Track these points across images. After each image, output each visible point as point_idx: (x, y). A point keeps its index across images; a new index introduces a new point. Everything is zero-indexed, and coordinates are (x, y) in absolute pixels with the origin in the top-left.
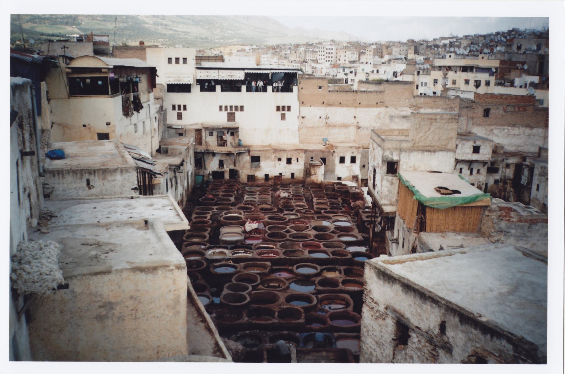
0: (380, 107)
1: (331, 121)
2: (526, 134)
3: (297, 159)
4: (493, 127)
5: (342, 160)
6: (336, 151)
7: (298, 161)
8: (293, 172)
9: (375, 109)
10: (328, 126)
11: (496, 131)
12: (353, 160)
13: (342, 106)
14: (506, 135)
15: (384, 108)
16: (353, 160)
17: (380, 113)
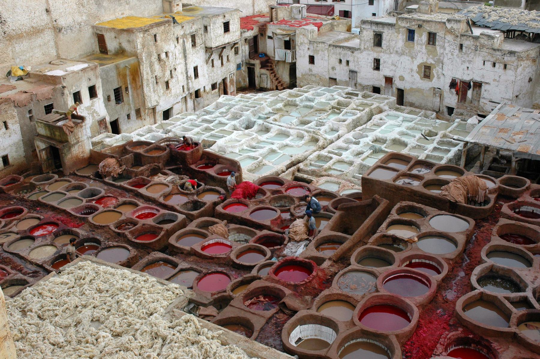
3: (5, 123)
5: (77, 97)
6: (65, 85)
7: (7, 128)
8: (4, 154)
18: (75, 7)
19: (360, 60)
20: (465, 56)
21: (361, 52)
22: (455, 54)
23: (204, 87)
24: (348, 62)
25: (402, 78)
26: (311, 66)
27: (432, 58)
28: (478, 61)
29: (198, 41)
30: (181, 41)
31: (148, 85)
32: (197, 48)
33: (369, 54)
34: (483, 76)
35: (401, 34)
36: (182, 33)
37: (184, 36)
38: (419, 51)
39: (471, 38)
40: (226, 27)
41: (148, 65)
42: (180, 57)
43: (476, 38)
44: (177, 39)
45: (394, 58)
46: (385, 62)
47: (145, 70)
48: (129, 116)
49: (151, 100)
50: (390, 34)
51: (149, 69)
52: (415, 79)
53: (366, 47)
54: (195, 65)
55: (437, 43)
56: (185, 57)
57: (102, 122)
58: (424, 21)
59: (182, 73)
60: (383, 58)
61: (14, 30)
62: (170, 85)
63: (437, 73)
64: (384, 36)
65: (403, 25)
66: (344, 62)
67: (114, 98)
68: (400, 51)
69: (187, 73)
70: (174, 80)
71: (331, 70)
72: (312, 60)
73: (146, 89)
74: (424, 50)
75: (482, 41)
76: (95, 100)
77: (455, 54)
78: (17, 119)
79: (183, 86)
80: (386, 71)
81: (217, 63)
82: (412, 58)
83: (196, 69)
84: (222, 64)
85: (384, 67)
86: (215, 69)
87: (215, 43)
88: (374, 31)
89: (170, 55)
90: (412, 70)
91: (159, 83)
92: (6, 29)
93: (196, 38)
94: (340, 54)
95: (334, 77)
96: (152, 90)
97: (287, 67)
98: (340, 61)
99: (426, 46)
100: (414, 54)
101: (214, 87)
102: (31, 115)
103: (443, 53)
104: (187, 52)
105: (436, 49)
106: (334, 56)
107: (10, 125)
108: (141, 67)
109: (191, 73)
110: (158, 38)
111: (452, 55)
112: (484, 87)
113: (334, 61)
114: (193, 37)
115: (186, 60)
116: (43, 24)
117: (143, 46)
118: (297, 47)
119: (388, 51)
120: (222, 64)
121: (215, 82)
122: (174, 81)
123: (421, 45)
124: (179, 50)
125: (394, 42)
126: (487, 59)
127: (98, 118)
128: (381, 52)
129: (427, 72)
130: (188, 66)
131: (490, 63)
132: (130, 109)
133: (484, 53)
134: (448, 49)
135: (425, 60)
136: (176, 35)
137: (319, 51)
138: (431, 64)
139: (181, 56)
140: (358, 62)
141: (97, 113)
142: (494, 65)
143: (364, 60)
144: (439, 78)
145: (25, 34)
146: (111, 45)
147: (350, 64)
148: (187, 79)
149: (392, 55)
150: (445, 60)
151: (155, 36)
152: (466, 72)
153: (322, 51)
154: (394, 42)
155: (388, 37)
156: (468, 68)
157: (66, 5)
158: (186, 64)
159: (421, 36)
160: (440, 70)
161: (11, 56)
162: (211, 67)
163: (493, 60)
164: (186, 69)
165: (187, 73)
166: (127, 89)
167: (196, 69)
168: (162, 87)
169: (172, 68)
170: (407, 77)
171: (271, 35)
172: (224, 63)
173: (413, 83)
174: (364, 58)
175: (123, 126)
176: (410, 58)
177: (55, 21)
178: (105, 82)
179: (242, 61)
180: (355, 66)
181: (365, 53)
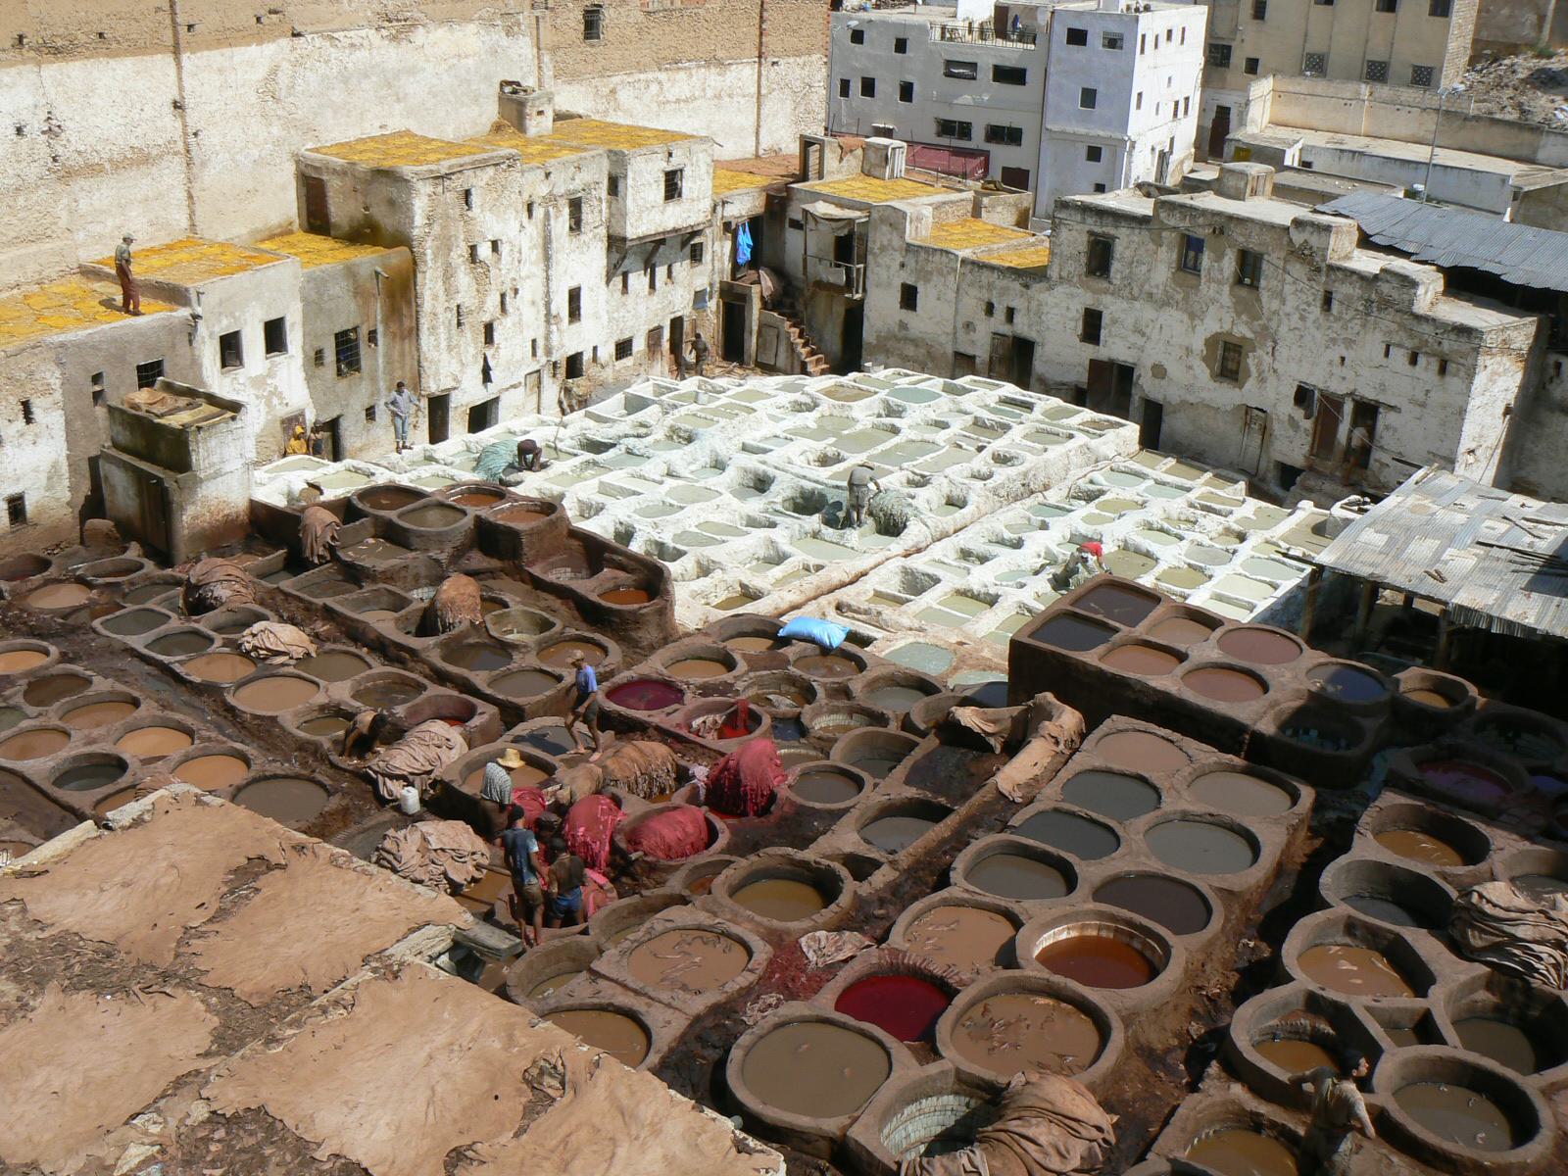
0: (274, 38)
1: (76, 141)
2: (710, 93)
3: (26, 407)
4: (615, 80)
5: (230, 348)
6: (199, 310)
7: (29, 419)
9: (253, 50)
10: (63, 172)
11: (625, 96)
12: (275, 336)
13: (112, 54)
14: (654, 106)
15: (285, 42)
16: (275, 336)
17: (274, 72)
18: (253, 99)
19: (1045, 309)
20: (1337, 326)
21: (1051, 288)
22: (1312, 317)
23: (595, 349)
24: (1010, 313)
25: (1159, 371)
26: (906, 315)
27: (1247, 323)
28: (1372, 344)
29: (588, 216)
30: (539, 212)
31: (433, 329)
32: (583, 237)
33: (1072, 295)
34: (1383, 388)
35: (1164, 248)
36: (543, 190)
37: (551, 199)
38: (1213, 301)
39: (1355, 277)
40: (672, 187)
41: (440, 273)
42: (533, 258)
43: (1369, 281)
44: (530, 208)
45: (1146, 312)
46: (1114, 321)
47: (429, 285)
48: (370, 413)
49: (437, 373)
50: (1134, 246)
51: (440, 283)
52: (1195, 377)
53: (1064, 274)
54: (574, 284)
55: (1263, 283)
56: (547, 258)
57: (290, 423)
58: (1231, 218)
59: (533, 303)
60: (1112, 308)
61: (80, 153)
62: (496, 336)
63: (1259, 364)
64: (1120, 249)
65: (1172, 222)
66: (1000, 313)
67: (334, 358)
68: (1158, 293)
69: (548, 305)
70: (508, 321)
71: (961, 333)
72: (909, 297)
73: (426, 339)
74: (1226, 298)
75: (1385, 288)
76: (279, 358)
77: (1312, 317)
78: (58, 396)
79: (534, 341)
80: (1114, 347)
81: (638, 280)
82: (1192, 316)
83: (574, 296)
84: (652, 286)
85: (1110, 336)
86: (630, 299)
87: (637, 227)
88: (1091, 233)
89: (504, 249)
90: (1189, 350)
91: (466, 328)
92: (60, 150)
93: (585, 208)
94: (990, 286)
95: (970, 351)
96: (444, 345)
97: (839, 310)
98: (990, 309)
99: (1231, 288)
100: (1196, 307)
101: (623, 349)
102: (97, 388)
103: (1276, 313)
104: (554, 245)
105: (1259, 300)
106: (973, 292)
107: (37, 413)
108: (419, 276)
109: (561, 305)
110: (475, 199)
111: (1302, 318)
112: (1384, 419)
113: (972, 305)
114: (576, 205)
115: (548, 268)
116: (160, 142)
117: (430, 220)
118: (870, 258)
119: (1126, 293)
120: (652, 286)
121: (626, 336)
122: (509, 325)
123: (1220, 283)
124: (532, 239)
125: (1144, 268)
126: (1396, 339)
127: (283, 412)
128: (1106, 292)
129: (1228, 359)
130: (553, 285)
131: (1403, 351)
132: (375, 393)
133: (1388, 321)
134: (1292, 302)
135: (1227, 327)
136: (526, 197)
137: (931, 273)
138: (1244, 338)
139: (534, 255)
140: (1039, 314)
141: (280, 396)
142: (1413, 360)
143: (1055, 310)
144: (1262, 380)
145: (107, 166)
146: (341, 208)
147: (1017, 319)
148: (548, 322)
149: (1137, 304)
150: (1283, 330)
151: (467, 194)
152: (1338, 370)
153: (940, 273)
154: (1144, 268)
155: (1128, 253)
156: (1343, 359)
157: (230, 93)
158: (548, 279)
159: (1220, 257)
160: (1268, 359)
161: (63, 223)
162: (619, 293)
163: (1409, 343)
164: (548, 294)
165: (548, 305)
166: (372, 337)
167: (574, 296)
168: (475, 340)
169: (507, 288)
170: (1174, 369)
171: (799, 217)
172: (658, 284)
173: (1189, 388)
174: (1057, 305)
175: (350, 437)
176: (1185, 318)
177: (195, 134)
178: (313, 307)
179: (711, 285)
180: (1030, 326)
181: (1061, 290)
